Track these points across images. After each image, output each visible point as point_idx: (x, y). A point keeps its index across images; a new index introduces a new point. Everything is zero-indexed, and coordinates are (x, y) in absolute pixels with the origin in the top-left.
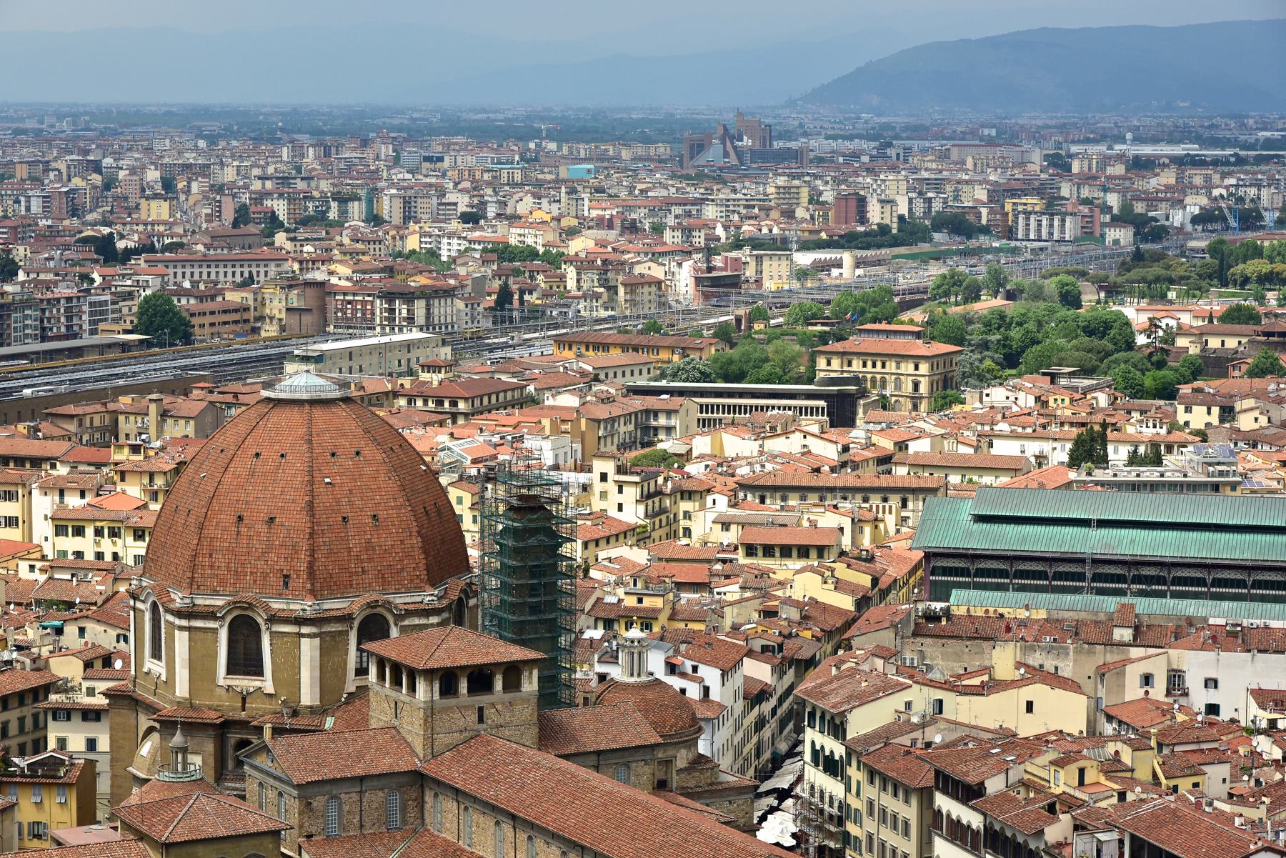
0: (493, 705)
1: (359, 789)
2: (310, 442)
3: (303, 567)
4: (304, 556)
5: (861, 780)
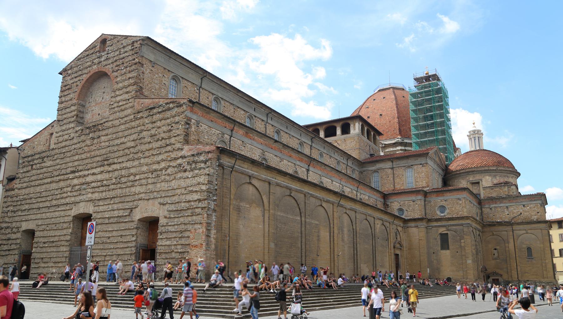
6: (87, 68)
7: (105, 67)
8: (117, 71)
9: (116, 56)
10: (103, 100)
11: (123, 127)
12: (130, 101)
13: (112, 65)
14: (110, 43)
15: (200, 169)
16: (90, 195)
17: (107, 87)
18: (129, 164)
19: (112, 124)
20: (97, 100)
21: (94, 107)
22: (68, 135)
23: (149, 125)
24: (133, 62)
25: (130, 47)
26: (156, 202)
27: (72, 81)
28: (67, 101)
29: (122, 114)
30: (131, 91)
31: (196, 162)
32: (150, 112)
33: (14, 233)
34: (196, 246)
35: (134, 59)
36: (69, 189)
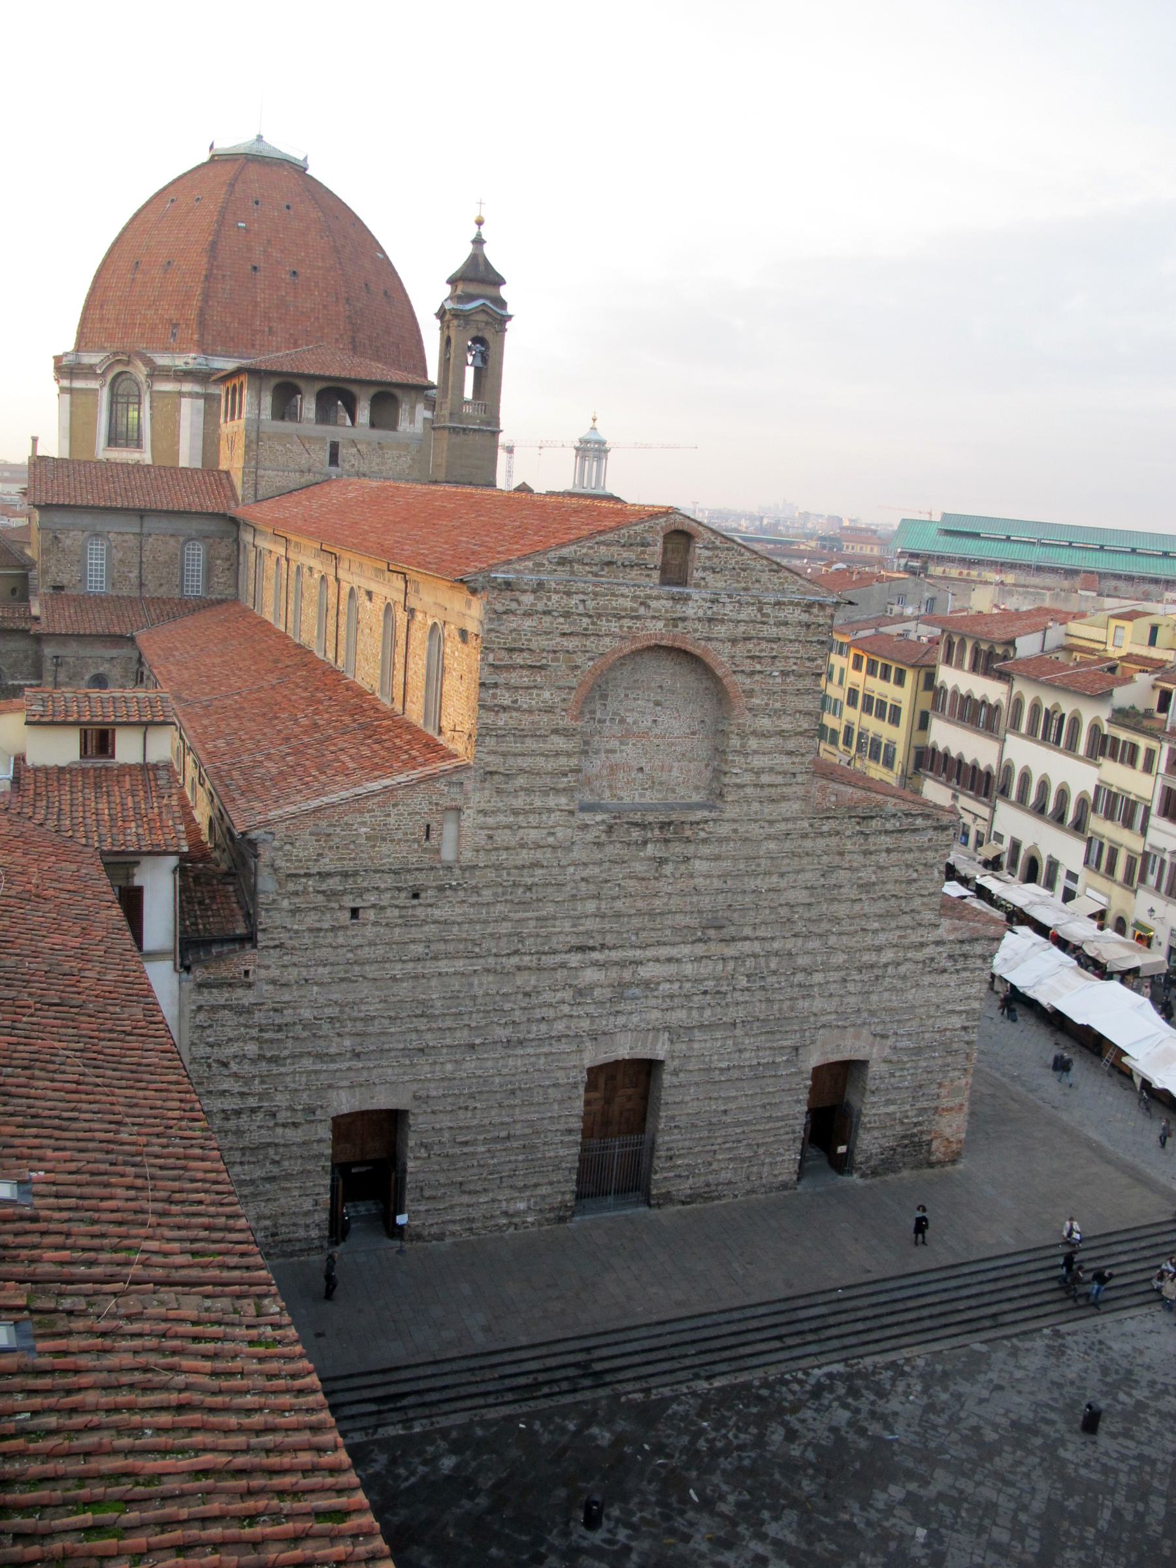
0: (354, 443)
1: (137, 530)
2: (232, 185)
3: (192, 315)
4: (196, 303)
5: (845, 666)
6: (621, 618)
7: (703, 643)
10: (657, 731)
11: (772, 845)
12: (799, 779)
14: (709, 558)
15: (973, 971)
16: (655, 1014)
17: (673, 692)
18: (790, 944)
19: (735, 831)
20: (628, 720)
21: (614, 744)
22: (545, 831)
23: (856, 856)
24: (808, 664)
25: (798, 615)
26: (865, 1032)
27: (545, 643)
28: (530, 712)
29: (768, 808)
30: (804, 751)
31: (965, 956)
32: (858, 823)
33: (284, 1125)
34: (952, 1109)
36: (567, 995)
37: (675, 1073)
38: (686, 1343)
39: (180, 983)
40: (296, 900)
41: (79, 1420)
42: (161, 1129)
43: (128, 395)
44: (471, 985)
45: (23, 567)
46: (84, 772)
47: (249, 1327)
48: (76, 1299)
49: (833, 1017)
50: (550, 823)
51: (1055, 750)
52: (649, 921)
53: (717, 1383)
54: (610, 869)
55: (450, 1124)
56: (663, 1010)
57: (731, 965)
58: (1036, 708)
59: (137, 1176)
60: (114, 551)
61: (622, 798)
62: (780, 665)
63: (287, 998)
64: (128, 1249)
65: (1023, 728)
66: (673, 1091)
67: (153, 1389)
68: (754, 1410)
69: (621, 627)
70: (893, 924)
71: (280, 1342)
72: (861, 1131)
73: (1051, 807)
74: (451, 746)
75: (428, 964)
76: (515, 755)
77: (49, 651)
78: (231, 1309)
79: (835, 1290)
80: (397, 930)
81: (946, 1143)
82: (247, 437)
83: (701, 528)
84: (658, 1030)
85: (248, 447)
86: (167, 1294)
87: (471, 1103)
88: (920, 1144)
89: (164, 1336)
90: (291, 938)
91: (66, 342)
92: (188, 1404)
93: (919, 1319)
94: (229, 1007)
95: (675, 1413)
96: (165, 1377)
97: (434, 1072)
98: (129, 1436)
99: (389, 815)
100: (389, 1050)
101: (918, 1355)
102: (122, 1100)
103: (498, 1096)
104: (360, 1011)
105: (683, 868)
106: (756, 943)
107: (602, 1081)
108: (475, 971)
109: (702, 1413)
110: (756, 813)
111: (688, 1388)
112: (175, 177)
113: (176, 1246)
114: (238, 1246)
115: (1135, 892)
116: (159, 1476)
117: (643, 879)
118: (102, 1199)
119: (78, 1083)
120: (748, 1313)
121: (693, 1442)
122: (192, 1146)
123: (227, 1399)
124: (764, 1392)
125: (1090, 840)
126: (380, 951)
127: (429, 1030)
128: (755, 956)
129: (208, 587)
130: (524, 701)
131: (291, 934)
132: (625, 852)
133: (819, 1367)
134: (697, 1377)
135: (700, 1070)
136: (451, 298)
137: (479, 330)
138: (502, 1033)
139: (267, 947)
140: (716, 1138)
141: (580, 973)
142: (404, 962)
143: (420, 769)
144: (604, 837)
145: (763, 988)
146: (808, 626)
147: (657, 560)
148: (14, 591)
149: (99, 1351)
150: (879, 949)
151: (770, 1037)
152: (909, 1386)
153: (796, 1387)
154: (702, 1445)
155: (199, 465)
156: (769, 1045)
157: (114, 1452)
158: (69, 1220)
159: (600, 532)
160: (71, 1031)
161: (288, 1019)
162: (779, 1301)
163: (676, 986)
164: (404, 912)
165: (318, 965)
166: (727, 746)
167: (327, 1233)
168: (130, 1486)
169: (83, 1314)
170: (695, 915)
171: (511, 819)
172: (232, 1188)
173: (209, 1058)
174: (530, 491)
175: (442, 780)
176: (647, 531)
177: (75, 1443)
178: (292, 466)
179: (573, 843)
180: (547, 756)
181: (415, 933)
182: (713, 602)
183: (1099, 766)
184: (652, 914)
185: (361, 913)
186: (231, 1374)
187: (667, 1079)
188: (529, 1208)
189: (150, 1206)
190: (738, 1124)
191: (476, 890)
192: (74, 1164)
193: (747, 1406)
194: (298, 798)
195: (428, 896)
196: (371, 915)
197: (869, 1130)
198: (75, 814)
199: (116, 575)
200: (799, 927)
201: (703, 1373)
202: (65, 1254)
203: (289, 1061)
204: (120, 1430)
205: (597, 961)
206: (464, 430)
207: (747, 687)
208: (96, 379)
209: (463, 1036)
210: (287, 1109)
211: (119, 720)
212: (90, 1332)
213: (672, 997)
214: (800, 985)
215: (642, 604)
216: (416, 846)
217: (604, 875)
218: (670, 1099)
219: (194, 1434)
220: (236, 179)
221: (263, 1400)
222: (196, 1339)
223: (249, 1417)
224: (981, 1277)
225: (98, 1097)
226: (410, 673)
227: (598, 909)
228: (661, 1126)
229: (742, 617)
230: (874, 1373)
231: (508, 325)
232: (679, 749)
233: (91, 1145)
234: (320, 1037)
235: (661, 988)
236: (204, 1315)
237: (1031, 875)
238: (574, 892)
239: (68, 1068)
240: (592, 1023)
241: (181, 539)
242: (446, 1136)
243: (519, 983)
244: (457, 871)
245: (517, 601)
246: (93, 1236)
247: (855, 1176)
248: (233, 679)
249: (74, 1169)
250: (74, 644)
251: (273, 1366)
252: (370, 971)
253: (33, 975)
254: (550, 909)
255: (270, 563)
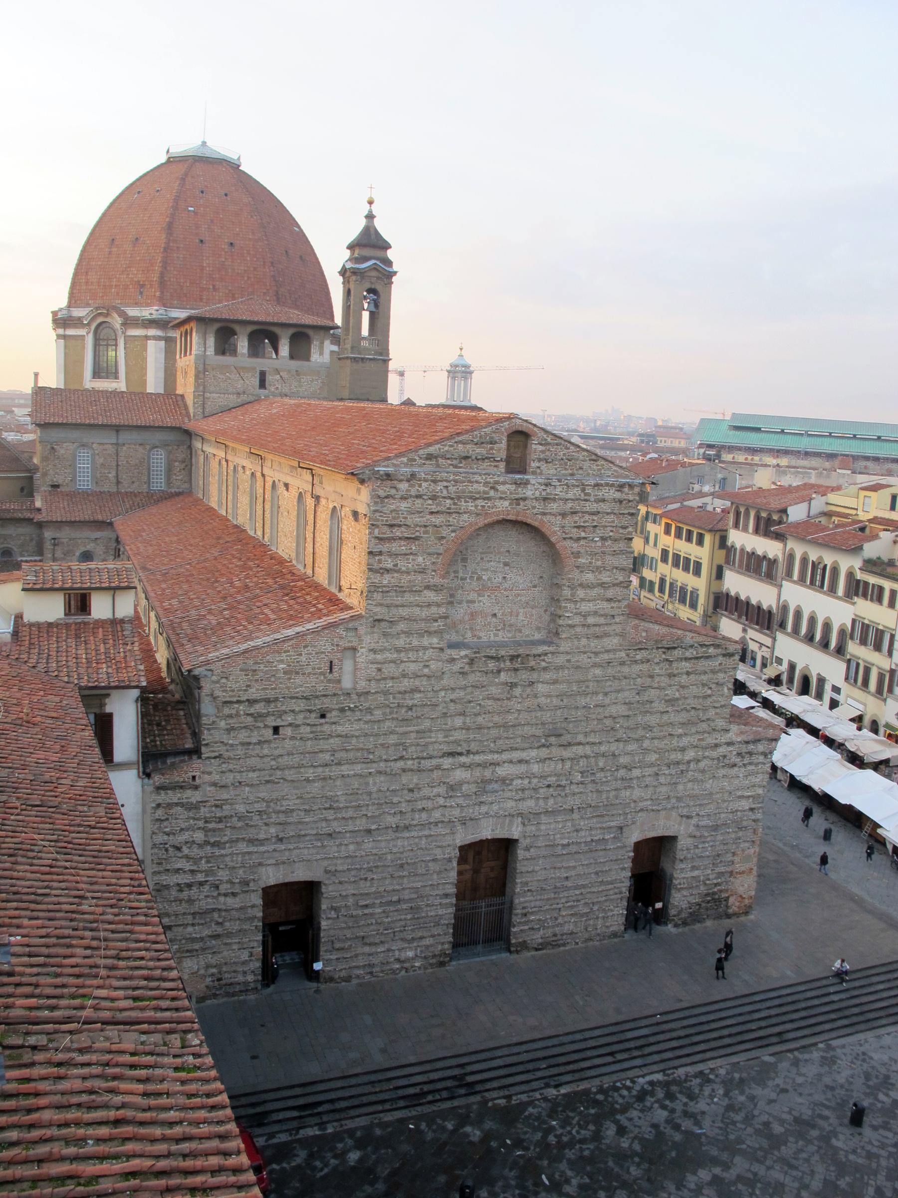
0: (277, 371)
1: (114, 441)
3: (155, 278)
5: (658, 532)
8: (579, 539)
9: (572, 500)
11: (598, 671)
12: (617, 620)
13: (559, 518)
14: (543, 452)
15: (757, 764)
16: (510, 804)
17: (518, 555)
18: (613, 747)
19: (569, 661)
20: (484, 577)
24: (621, 531)
25: (613, 494)
27: (418, 520)
28: (408, 573)
29: (594, 643)
30: (620, 598)
31: (750, 754)
32: (664, 653)
33: (225, 895)
34: (743, 872)
35: (625, 528)
36: (442, 790)
37: (527, 849)
38: (538, 1059)
39: (143, 786)
40: (231, 721)
41: (36, 1134)
42: (114, 901)
43: (108, 340)
44: (367, 784)
45: (29, 471)
46: (68, 626)
47: (175, 1056)
48: (39, 1037)
49: (649, 803)
50: (426, 658)
51: (820, 592)
52: (504, 731)
53: (563, 1090)
54: (472, 693)
55: (353, 892)
56: (516, 800)
57: (568, 765)
58: (804, 560)
59: (93, 939)
60: (97, 457)
61: (479, 638)
62: (600, 532)
63: (225, 796)
64: (84, 996)
65: (796, 576)
66: (525, 863)
67: (97, 1108)
68: (592, 1111)
69: (476, 506)
70: (693, 730)
71: (199, 1068)
72: (673, 891)
73: (818, 636)
74: (348, 601)
75: (334, 768)
76: (397, 606)
77: (48, 534)
78: (162, 1043)
79: (655, 1015)
80: (309, 743)
81: (739, 899)
82: (196, 368)
83: (535, 429)
84: (513, 816)
85: (197, 377)
86: (112, 1032)
87: (370, 875)
88: (719, 900)
89: (107, 1065)
90: (227, 751)
91: (61, 301)
92: (123, 1119)
93: (721, 1038)
94: (182, 805)
95: (531, 1115)
96: (106, 1097)
97: (339, 852)
98: (75, 1146)
99: (301, 655)
100: (305, 835)
101: (721, 1066)
102: (85, 879)
103: (390, 869)
104: (282, 806)
105: (528, 690)
106: (587, 747)
107: (471, 857)
108: (370, 773)
109: (553, 1113)
110: (584, 647)
111: (541, 1094)
112: (141, 174)
113: (121, 993)
114: (170, 993)
115: (885, 700)
116: (97, 1178)
117: (498, 699)
118: (65, 957)
119: (51, 866)
120: (588, 1034)
121: (545, 1137)
122: (138, 914)
123: (154, 1114)
124: (600, 1097)
125: (849, 662)
126: (296, 759)
127: (335, 819)
128: (587, 757)
129: (169, 482)
130: (402, 564)
131: (228, 747)
132: (484, 679)
133: (643, 1076)
134: (547, 1086)
135: (546, 846)
136: (350, 260)
137: (372, 283)
138: (391, 821)
139: (208, 758)
140: (560, 898)
141: (451, 773)
142: (315, 767)
143: (325, 618)
144: (467, 668)
145: (593, 781)
146: (621, 502)
147: (503, 454)
148: (22, 489)
149: (54, 1078)
150: (683, 750)
151: (601, 819)
152: (713, 1090)
153: (625, 1092)
154: (552, 1139)
155: (162, 392)
156: (600, 825)
157: (62, 1159)
158: (38, 974)
159: (458, 434)
160: (48, 826)
161: (226, 813)
162: (611, 1025)
163: (526, 781)
164: (314, 729)
165: (249, 771)
166: (561, 596)
167: (260, 978)
168: (72, 1187)
169: (44, 1049)
170: (539, 727)
171: (395, 656)
172: (167, 947)
173: (166, 844)
174: (414, 404)
175: (341, 627)
176: (494, 432)
177: (31, 1152)
178: (231, 390)
179: (443, 673)
180: (421, 606)
181: (323, 745)
182: (546, 485)
183: (854, 604)
184: (505, 726)
185: (281, 731)
186: (159, 1094)
187: (521, 853)
188: (416, 956)
189: (102, 962)
190: (577, 887)
191: (369, 711)
192: (45, 930)
193: (586, 1108)
194: (231, 643)
195: (332, 716)
196: (289, 732)
197: (679, 890)
198: (60, 659)
199: (98, 475)
200: (620, 734)
201: (552, 1083)
202: (33, 1001)
203: (227, 845)
204: (67, 1141)
205: (464, 763)
206: (362, 359)
207: (575, 550)
208: (83, 328)
209: (361, 824)
210: (227, 882)
211: (93, 586)
212: (49, 1063)
213: (523, 790)
214: (622, 779)
215: (492, 488)
216: (322, 678)
217: (469, 697)
218: (524, 869)
219: (127, 1143)
220: (186, 175)
221: (183, 1115)
222: (133, 1066)
223: (171, 1128)
224: (769, 1004)
225: (66, 877)
226: (317, 545)
227: (464, 723)
228: (518, 890)
229: (570, 495)
230: (686, 1081)
231: (394, 279)
232: (523, 599)
233: (58, 915)
234: (252, 826)
235: (514, 783)
236: (140, 1047)
237: (805, 689)
238: (445, 711)
239: (43, 855)
240: (461, 812)
241: (148, 447)
242: (351, 901)
243: (404, 782)
244: (354, 696)
245: (395, 488)
246: (56, 987)
247: (670, 926)
248: (186, 552)
249: (44, 934)
250: (67, 528)
251: (192, 1087)
252: (290, 775)
253: (20, 783)
254: (427, 724)
255: (214, 464)
